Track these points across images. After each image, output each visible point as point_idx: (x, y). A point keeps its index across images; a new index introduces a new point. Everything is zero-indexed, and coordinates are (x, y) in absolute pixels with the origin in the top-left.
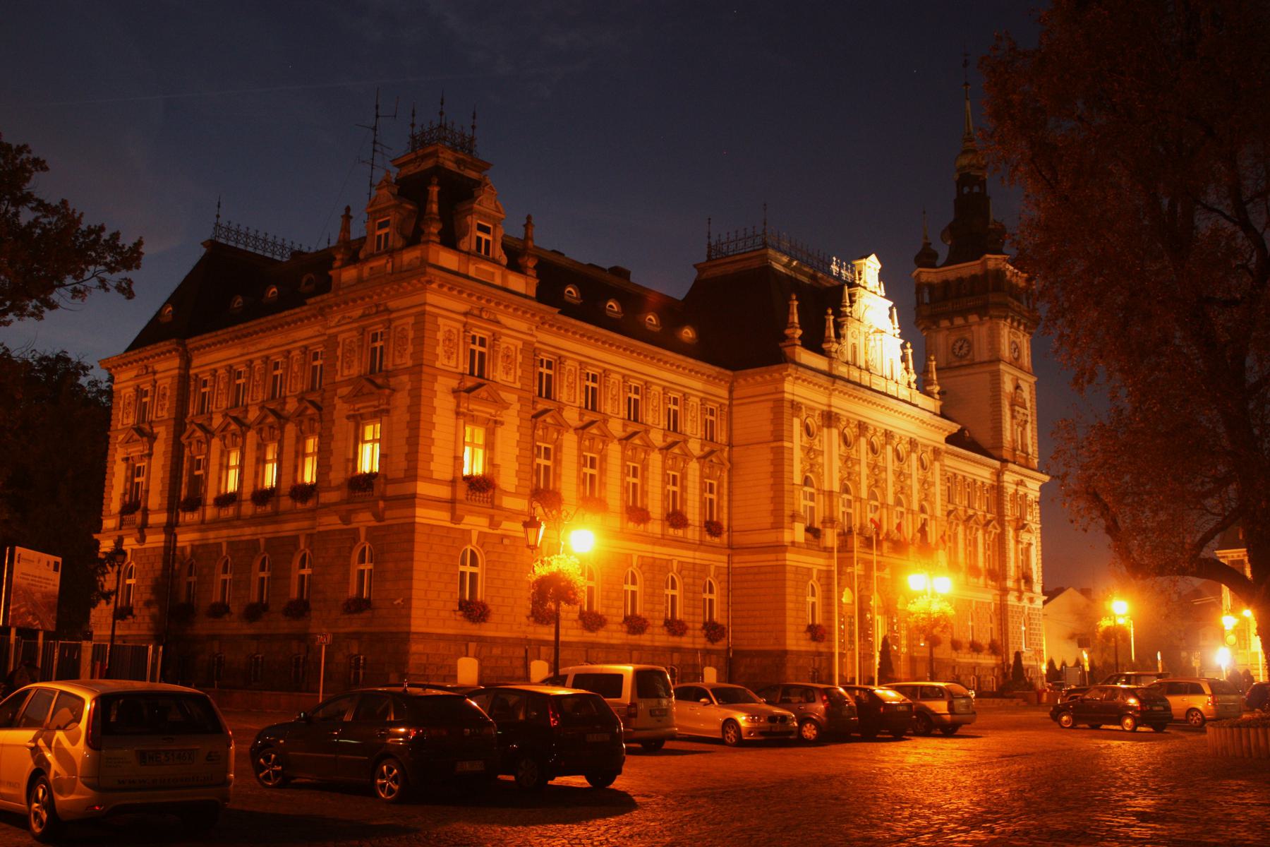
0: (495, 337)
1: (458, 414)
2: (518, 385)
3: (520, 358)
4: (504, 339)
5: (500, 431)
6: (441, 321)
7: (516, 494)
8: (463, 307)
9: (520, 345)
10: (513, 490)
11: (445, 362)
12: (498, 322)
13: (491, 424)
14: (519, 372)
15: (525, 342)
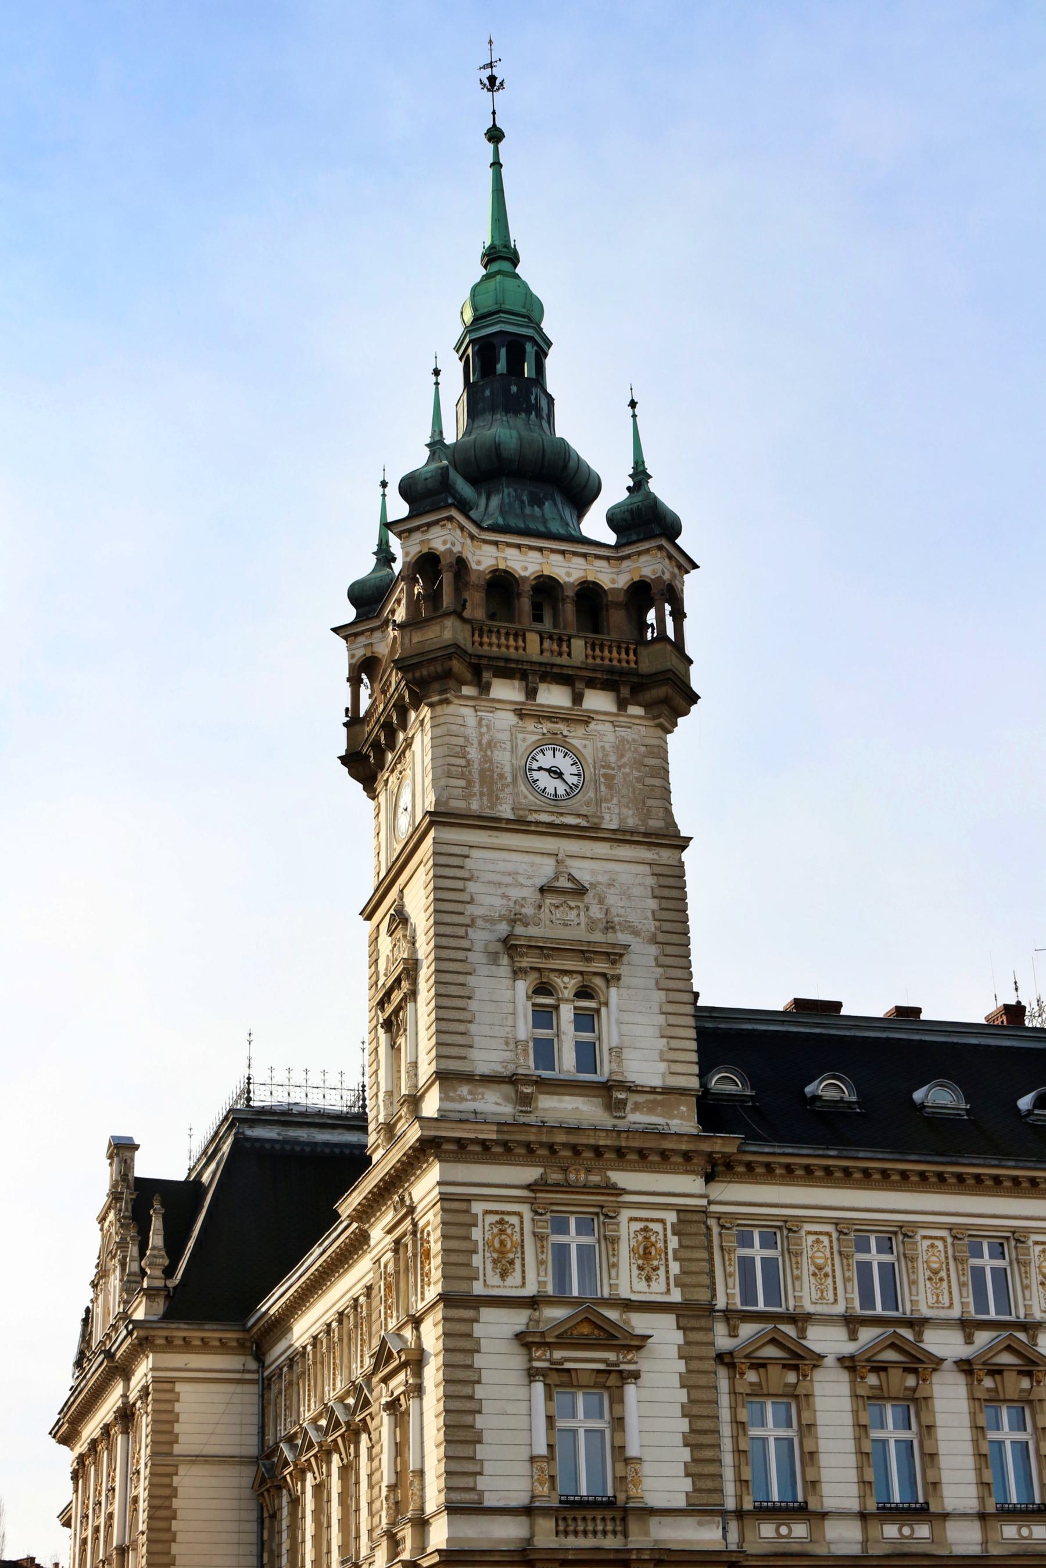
0: (609, 1215)
1: (532, 1374)
2: (676, 1296)
3: (674, 1242)
4: (625, 1214)
5: (631, 1391)
6: (477, 1208)
7: (695, 1510)
8: (530, 1174)
9: (671, 1217)
10: (681, 1502)
11: (494, 1279)
12: (614, 1187)
13: (613, 1381)
14: (675, 1268)
15: (680, 1211)
